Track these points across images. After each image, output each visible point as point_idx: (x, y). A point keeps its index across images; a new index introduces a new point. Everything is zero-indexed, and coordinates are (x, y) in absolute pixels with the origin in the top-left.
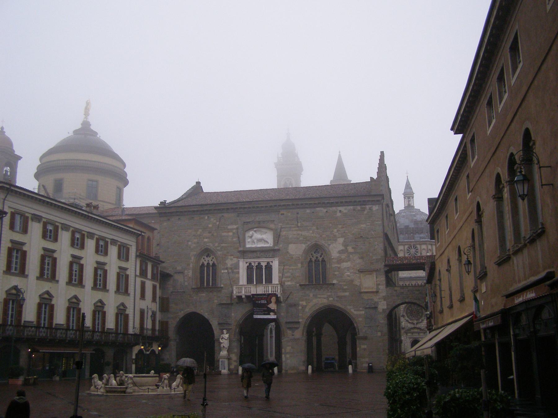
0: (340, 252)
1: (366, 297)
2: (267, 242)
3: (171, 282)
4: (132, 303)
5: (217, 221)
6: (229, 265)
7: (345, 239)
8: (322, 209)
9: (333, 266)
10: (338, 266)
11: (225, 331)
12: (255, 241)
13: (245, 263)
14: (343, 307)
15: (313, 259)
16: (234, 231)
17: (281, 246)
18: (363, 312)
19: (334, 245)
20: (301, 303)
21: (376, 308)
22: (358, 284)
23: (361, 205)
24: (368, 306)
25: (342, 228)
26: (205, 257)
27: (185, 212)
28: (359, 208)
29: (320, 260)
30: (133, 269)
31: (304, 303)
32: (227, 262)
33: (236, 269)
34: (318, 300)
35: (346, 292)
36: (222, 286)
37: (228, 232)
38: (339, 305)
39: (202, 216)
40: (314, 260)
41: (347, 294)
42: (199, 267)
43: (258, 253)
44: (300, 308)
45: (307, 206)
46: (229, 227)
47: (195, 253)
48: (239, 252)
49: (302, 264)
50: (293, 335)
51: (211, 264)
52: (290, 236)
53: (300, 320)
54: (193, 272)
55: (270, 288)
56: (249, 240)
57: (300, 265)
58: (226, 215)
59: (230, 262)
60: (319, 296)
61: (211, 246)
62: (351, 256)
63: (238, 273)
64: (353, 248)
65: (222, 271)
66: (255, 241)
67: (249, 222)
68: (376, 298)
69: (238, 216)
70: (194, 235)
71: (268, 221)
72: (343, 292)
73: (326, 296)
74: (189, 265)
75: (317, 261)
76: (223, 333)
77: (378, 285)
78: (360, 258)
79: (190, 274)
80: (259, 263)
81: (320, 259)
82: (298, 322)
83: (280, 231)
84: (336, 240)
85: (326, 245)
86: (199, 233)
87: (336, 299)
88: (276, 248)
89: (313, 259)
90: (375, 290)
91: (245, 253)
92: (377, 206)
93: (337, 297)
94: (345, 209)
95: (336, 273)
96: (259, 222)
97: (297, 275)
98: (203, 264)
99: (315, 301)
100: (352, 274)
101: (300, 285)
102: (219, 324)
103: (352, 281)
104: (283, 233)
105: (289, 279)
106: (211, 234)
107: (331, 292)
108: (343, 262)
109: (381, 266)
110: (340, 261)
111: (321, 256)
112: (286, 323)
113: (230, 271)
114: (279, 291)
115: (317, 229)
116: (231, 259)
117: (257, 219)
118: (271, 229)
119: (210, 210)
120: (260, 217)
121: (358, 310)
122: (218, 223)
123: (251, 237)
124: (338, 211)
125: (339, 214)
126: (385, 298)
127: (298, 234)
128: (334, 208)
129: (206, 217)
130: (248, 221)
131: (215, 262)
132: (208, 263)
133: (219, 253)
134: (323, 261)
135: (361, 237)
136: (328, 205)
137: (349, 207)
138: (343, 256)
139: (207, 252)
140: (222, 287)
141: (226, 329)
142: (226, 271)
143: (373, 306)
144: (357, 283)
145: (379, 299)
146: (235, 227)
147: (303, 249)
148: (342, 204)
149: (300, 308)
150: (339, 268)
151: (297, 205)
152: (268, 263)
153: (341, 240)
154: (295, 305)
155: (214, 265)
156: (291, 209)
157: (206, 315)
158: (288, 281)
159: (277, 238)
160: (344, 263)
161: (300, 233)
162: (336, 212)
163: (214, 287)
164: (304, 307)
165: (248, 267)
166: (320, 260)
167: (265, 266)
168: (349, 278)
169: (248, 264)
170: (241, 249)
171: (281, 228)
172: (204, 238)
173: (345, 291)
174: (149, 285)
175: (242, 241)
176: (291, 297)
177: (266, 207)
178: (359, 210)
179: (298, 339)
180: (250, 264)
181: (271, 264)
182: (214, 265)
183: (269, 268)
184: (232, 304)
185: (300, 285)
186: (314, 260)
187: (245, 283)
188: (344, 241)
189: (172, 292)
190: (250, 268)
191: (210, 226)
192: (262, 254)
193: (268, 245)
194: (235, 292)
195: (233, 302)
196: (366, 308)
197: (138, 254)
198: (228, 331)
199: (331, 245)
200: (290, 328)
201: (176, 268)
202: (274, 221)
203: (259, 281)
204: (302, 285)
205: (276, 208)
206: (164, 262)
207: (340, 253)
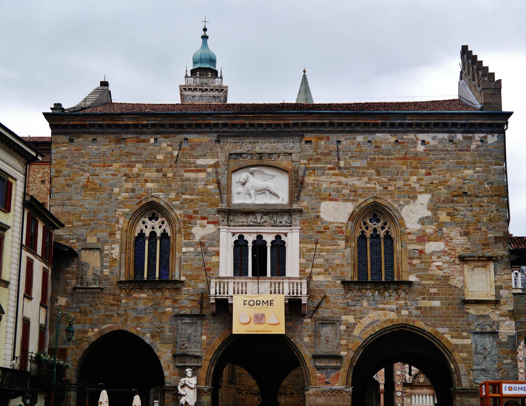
0: (422, 221)
1: (472, 310)
2: (278, 197)
3: (74, 267)
4: (13, 304)
5: (175, 150)
6: (197, 238)
7: (433, 195)
8: (388, 136)
9: (410, 247)
10: (419, 247)
11: (189, 371)
12: (252, 192)
13: (231, 235)
14: (429, 329)
15: (368, 233)
16: (209, 170)
17: (304, 203)
18: (469, 341)
19: (411, 206)
20: (344, 318)
21: (494, 334)
22: (459, 285)
23: (463, 132)
24: (478, 330)
25: (429, 174)
26: (147, 220)
27: (109, 126)
28: (459, 136)
29: (382, 236)
30: (17, 229)
31: (351, 319)
32: (194, 230)
33: (212, 245)
34: (376, 314)
35: (434, 299)
36: (183, 278)
37: (198, 171)
38: (420, 324)
39: (143, 137)
40: (368, 236)
41: (436, 303)
42: (133, 239)
43: (259, 217)
44: (343, 327)
45: (358, 129)
46: (200, 162)
47: (127, 210)
48: (219, 211)
49: (347, 240)
50: (327, 383)
51: (159, 234)
52: (324, 186)
53: (343, 353)
54: (121, 249)
55: (286, 286)
56: (240, 189)
57: (342, 243)
58: (194, 138)
59: (199, 231)
60: (381, 306)
61: (162, 198)
62: (444, 229)
63: (217, 254)
64: (449, 214)
65: (184, 250)
66: (252, 192)
67: (240, 154)
68: (495, 315)
69: (218, 141)
70: (125, 175)
71: (279, 155)
72: (429, 299)
73: (394, 307)
74: (112, 234)
75: (375, 236)
76: (185, 376)
77: (498, 288)
78: (461, 235)
79: (116, 252)
80: (260, 237)
81: (382, 233)
82: (339, 358)
83: (303, 177)
84: (415, 198)
85: (396, 206)
86: (135, 170)
87: (415, 312)
88: (295, 206)
89: (368, 233)
90: (493, 298)
91: (231, 213)
92: (496, 135)
93: (417, 308)
94: (434, 138)
95: (415, 262)
96: (261, 155)
97: (338, 262)
98: (142, 234)
99: (372, 316)
100: (446, 265)
101: (344, 283)
102: (175, 356)
103: (446, 278)
104: (309, 180)
105: (322, 270)
106: (161, 174)
107: (405, 299)
108: (429, 241)
109: (501, 251)
110: (423, 238)
111: (383, 228)
112: (316, 357)
113: (199, 249)
114: (305, 292)
115: (379, 174)
116: (203, 226)
117: (258, 149)
119: (162, 126)
120: (264, 146)
121: (460, 337)
122: (176, 153)
123: (244, 184)
124: (419, 142)
125: (421, 148)
126: (513, 315)
127: (340, 183)
128: (411, 136)
129: (152, 140)
130: (239, 151)
131: (168, 231)
132: (153, 234)
133: (178, 212)
134: (388, 237)
135: (465, 193)
136: (401, 129)
137: (440, 136)
138: (430, 230)
139: (152, 209)
140: (182, 282)
141: (190, 367)
142: (191, 249)
143: (489, 329)
144: (456, 282)
145: (501, 315)
146: (211, 161)
147: (351, 211)
148: (427, 128)
149: (343, 327)
150: (421, 252)
151: (340, 125)
152: (278, 237)
153: (424, 199)
154: (333, 322)
155: (164, 235)
156: (325, 132)
157: (148, 339)
158: (319, 274)
159: (297, 187)
160: (431, 243)
161: (343, 179)
162: (414, 143)
163: (166, 283)
164: (350, 327)
165: (235, 242)
166: (382, 236)
167: (272, 242)
168: (441, 273)
169: (236, 237)
170: (224, 206)
171: (306, 168)
172: (146, 181)
173: (432, 297)
174: (38, 266)
175: (224, 189)
176: (324, 305)
177: (278, 125)
178: (460, 141)
179: (339, 391)
180: (241, 237)
181: (283, 238)
182: (164, 235)
183: (279, 246)
184: (201, 316)
185: (344, 283)
186: (368, 236)
187: (230, 273)
188: (431, 200)
189: (75, 289)
190: (240, 245)
191: (160, 157)
192: (265, 218)
194: (213, 292)
195: (205, 312)
196: (475, 333)
197: (28, 198)
198: (195, 370)
199: (406, 207)
200: (318, 368)
201: (85, 240)
202: (290, 154)
203: (259, 272)
204: (349, 283)
205: (296, 129)
206: (62, 226)
207: (423, 224)
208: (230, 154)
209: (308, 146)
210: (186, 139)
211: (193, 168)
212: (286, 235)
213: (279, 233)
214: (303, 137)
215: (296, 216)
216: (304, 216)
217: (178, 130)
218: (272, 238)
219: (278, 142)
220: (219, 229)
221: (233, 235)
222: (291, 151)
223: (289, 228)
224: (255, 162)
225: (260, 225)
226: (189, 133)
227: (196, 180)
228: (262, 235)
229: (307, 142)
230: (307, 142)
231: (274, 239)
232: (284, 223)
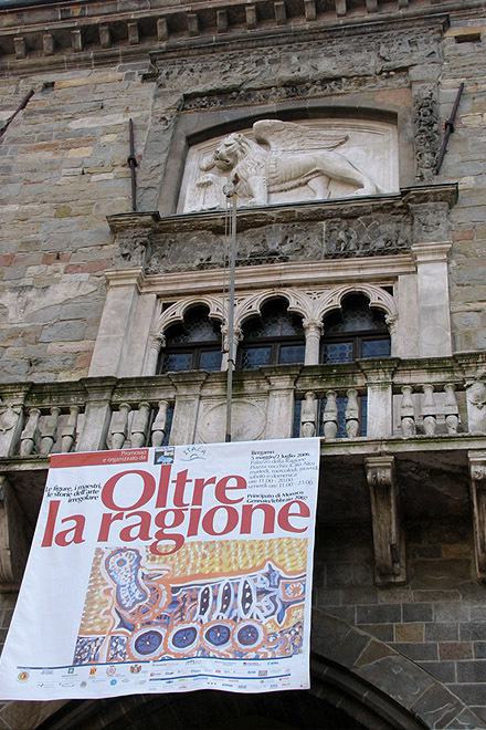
58: (71, 80)
96: (294, 86)
117: (285, 74)
118: (388, 117)
130: (217, 83)
152: (355, 302)
165: (173, 331)
169: (178, 310)
180: (198, 314)
181: (376, 296)
193: (361, 193)
202: (405, 69)
208: (187, 98)
209: (466, 47)
210: (49, 86)
211: (53, 141)
212: (390, 290)
213: (361, 281)
214: (447, 25)
215: (430, 213)
216: (461, 216)
217: (26, 61)
218: (331, 299)
219: (358, 50)
220: (108, 283)
221: (166, 306)
222: (406, 63)
223: (401, 257)
224: (272, 106)
225: (272, 257)
226: (57, 67)
227: (53, 167)
228: (286, 292)
229: (460, 39)
230: (460, 39)
231: (337, 303)
232: (380, 244)
